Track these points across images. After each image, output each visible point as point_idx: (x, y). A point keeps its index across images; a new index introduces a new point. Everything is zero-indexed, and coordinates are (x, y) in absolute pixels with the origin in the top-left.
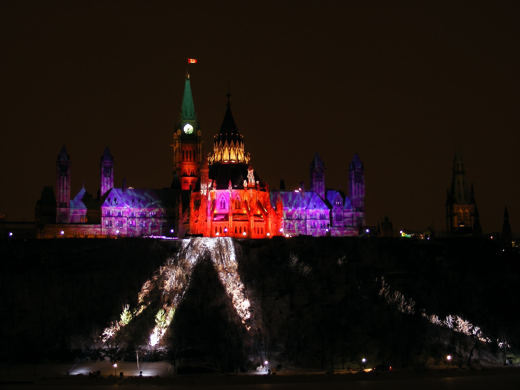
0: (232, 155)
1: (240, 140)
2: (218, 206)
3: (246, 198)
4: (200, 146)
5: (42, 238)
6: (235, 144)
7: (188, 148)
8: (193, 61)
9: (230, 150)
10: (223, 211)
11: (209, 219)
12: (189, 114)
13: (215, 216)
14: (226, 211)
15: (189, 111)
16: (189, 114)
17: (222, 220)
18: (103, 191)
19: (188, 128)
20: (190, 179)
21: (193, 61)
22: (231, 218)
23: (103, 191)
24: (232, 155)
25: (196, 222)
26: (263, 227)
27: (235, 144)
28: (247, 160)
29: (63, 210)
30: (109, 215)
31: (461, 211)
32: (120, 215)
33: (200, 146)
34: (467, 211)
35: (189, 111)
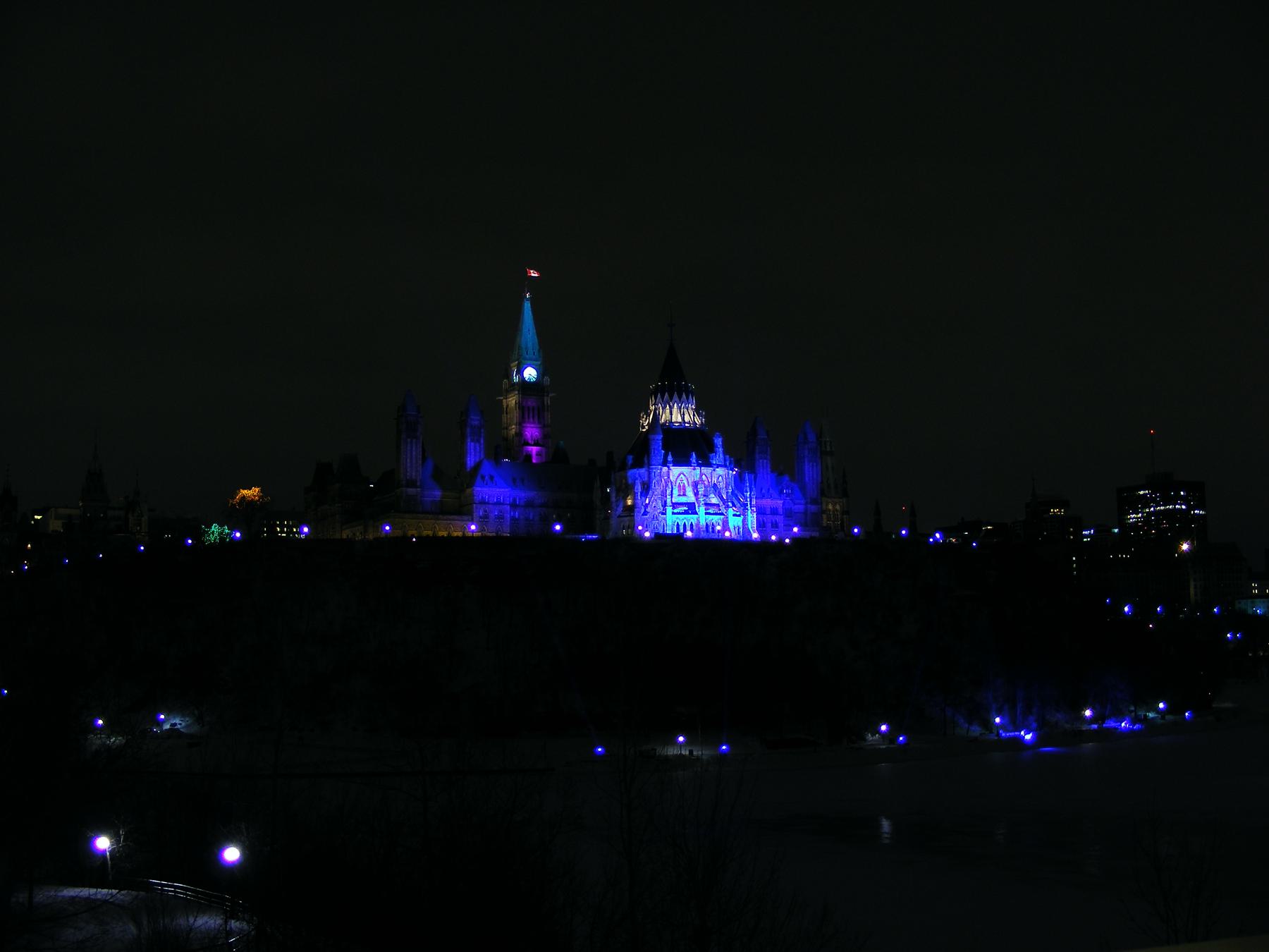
0: (680, 414)
1: (689, 392)
2: (676, 492)
3: (715, 480)
4: (547, 401)
5: (371, 537)
6: (680, 397)
7: (531, 402)
8: (534, 274)
9: (671, 408)
10: (683, 499)
11: (669, 510)
12: (530, 351)
13: (675, 505)
14: (690, 498)
15: (530, 345)
16: (530, 351)
17: (686, 513)
18: (470, 462)
19: (530, 373)
20: (534, 449)
21: (534, 274)
22: (701, 510)
23: (470, 462)
24: (680, 414)
25: (645, 513)
26: (741, 524)
27: (680, 397)
28: (698, 421)
29: (411, 491)
30: (483, 502)
31: (830, 507)
32: (498, 503)
33: (547, 401)
34: (838, 507)
35: (530, 345)
